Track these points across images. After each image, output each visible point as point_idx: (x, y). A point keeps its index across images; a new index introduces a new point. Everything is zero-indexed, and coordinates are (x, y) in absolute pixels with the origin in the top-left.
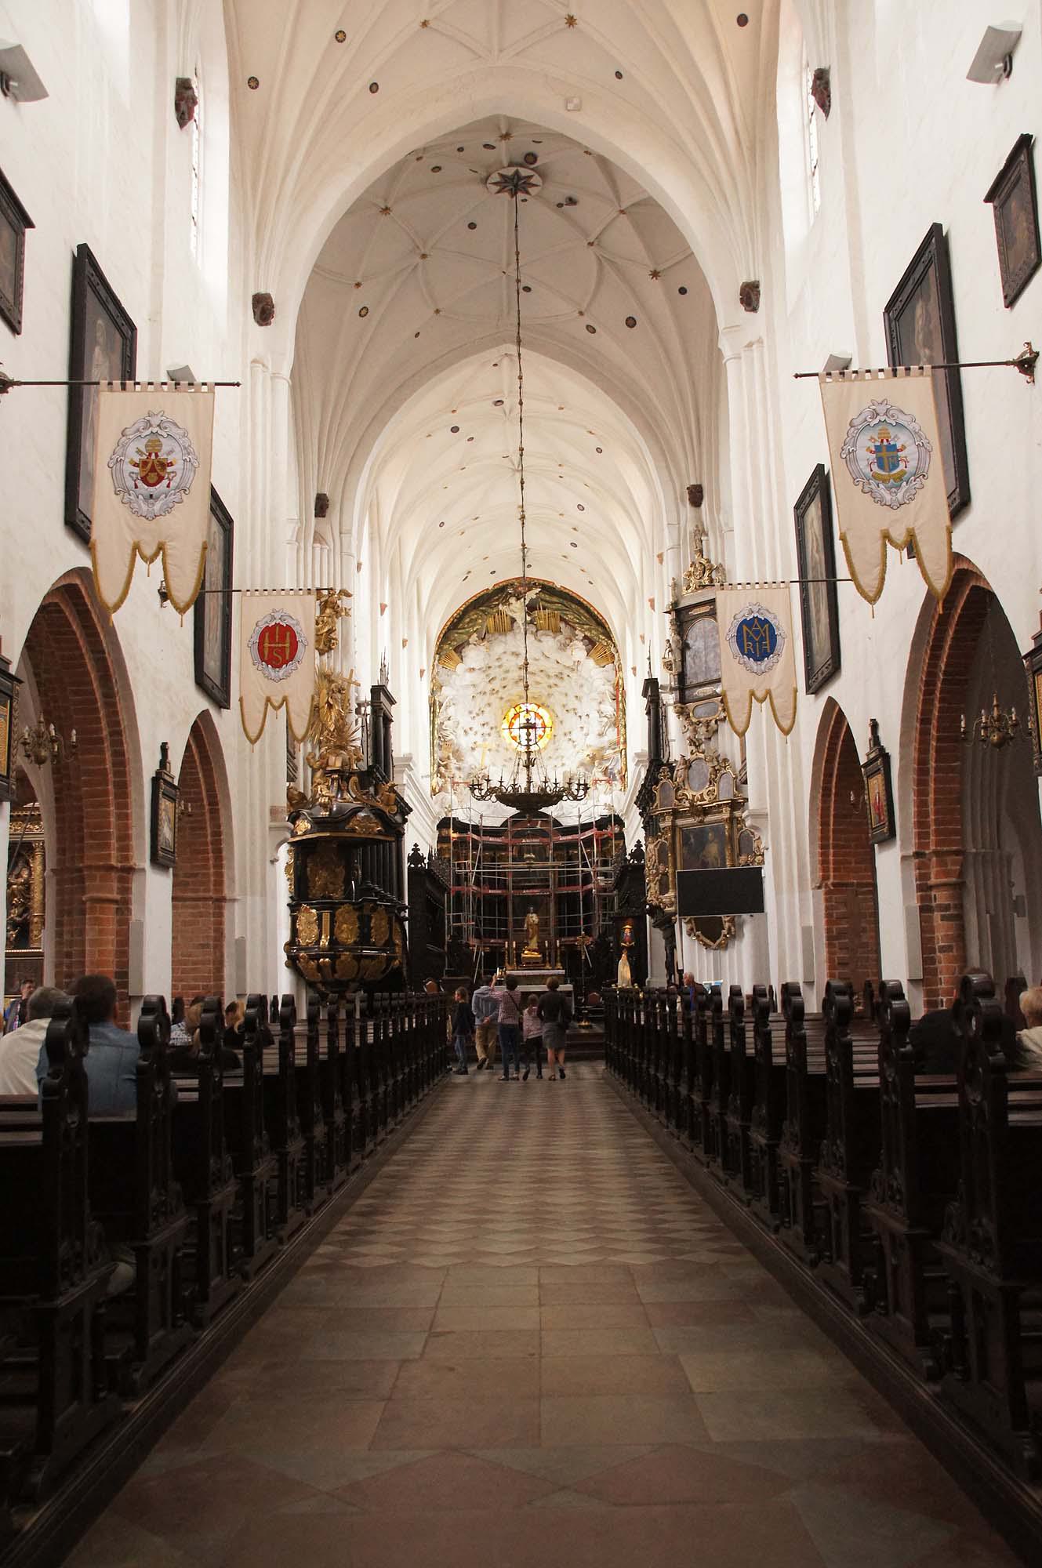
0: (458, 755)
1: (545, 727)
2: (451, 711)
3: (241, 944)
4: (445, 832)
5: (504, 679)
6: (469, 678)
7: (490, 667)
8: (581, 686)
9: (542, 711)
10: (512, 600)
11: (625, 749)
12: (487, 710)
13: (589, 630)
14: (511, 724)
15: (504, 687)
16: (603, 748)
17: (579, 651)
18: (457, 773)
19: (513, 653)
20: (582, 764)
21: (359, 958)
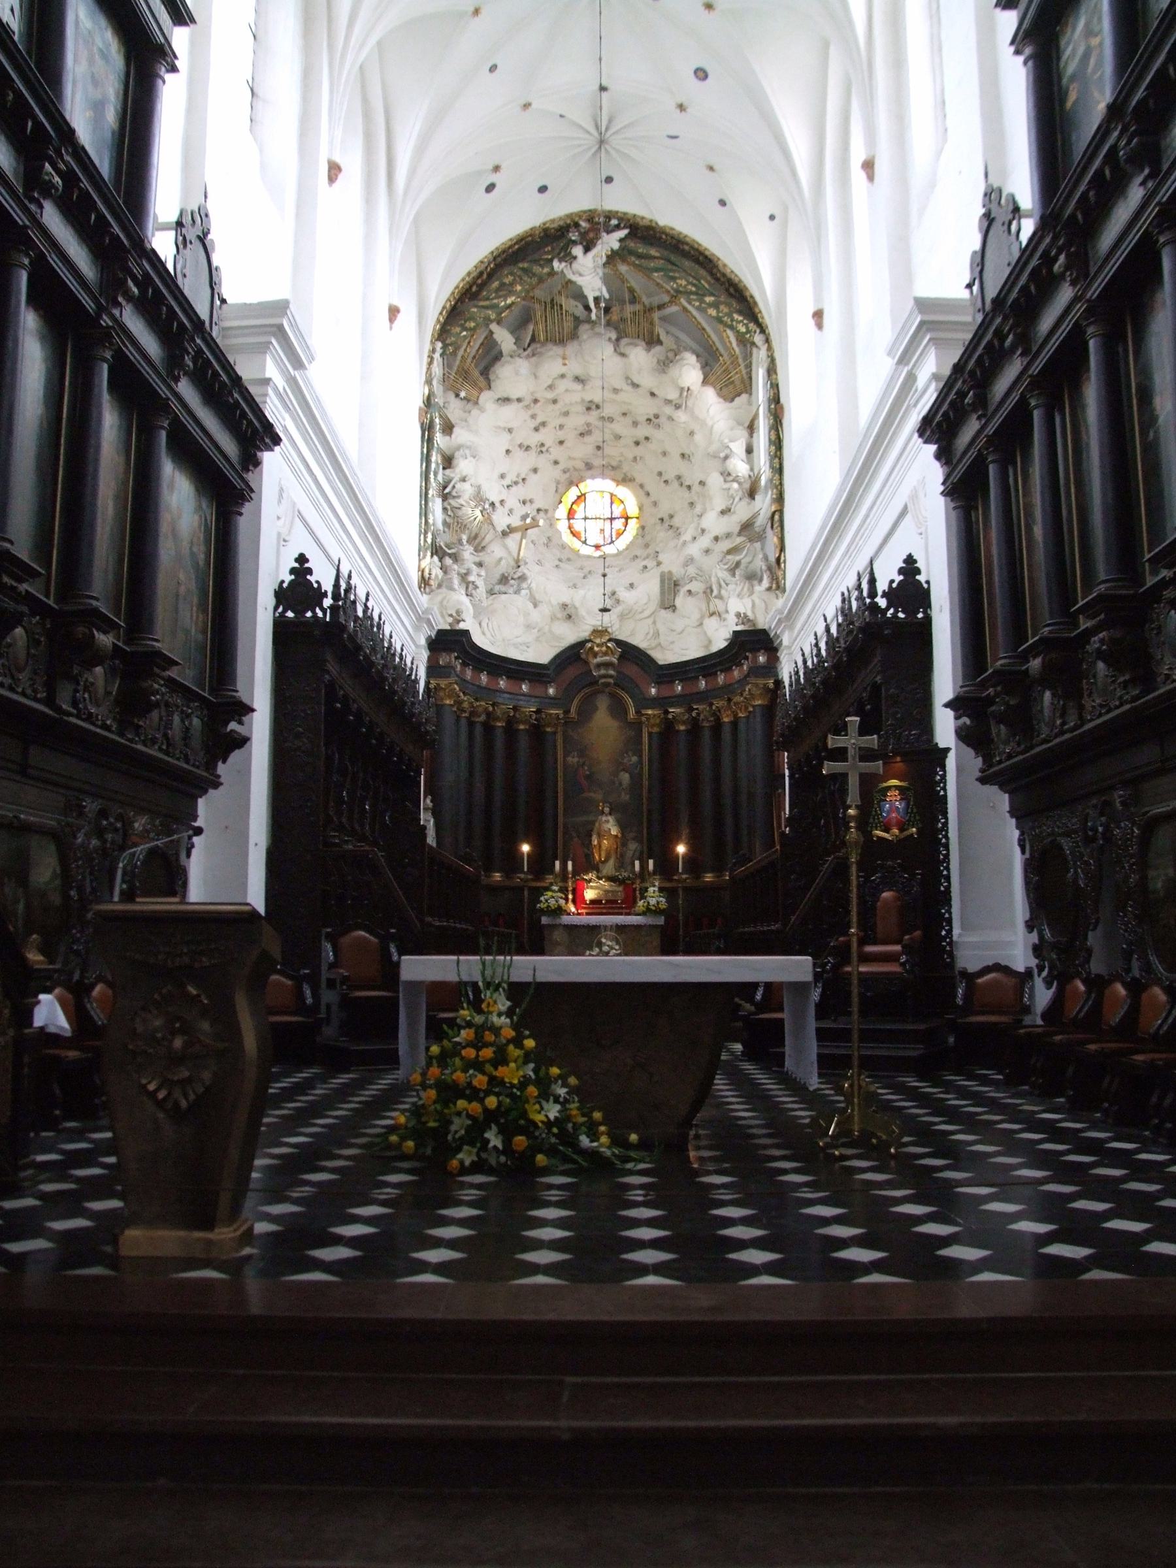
5: (561, 427)
7: (536, 401)
8: (692, 433)
9: (623, 492)
10: (577, 251)
11: (781, 511)
12: (533, 479)
13: (715, 305)
15: (561, 443)
17: (690, 373)
19: (577, 379)
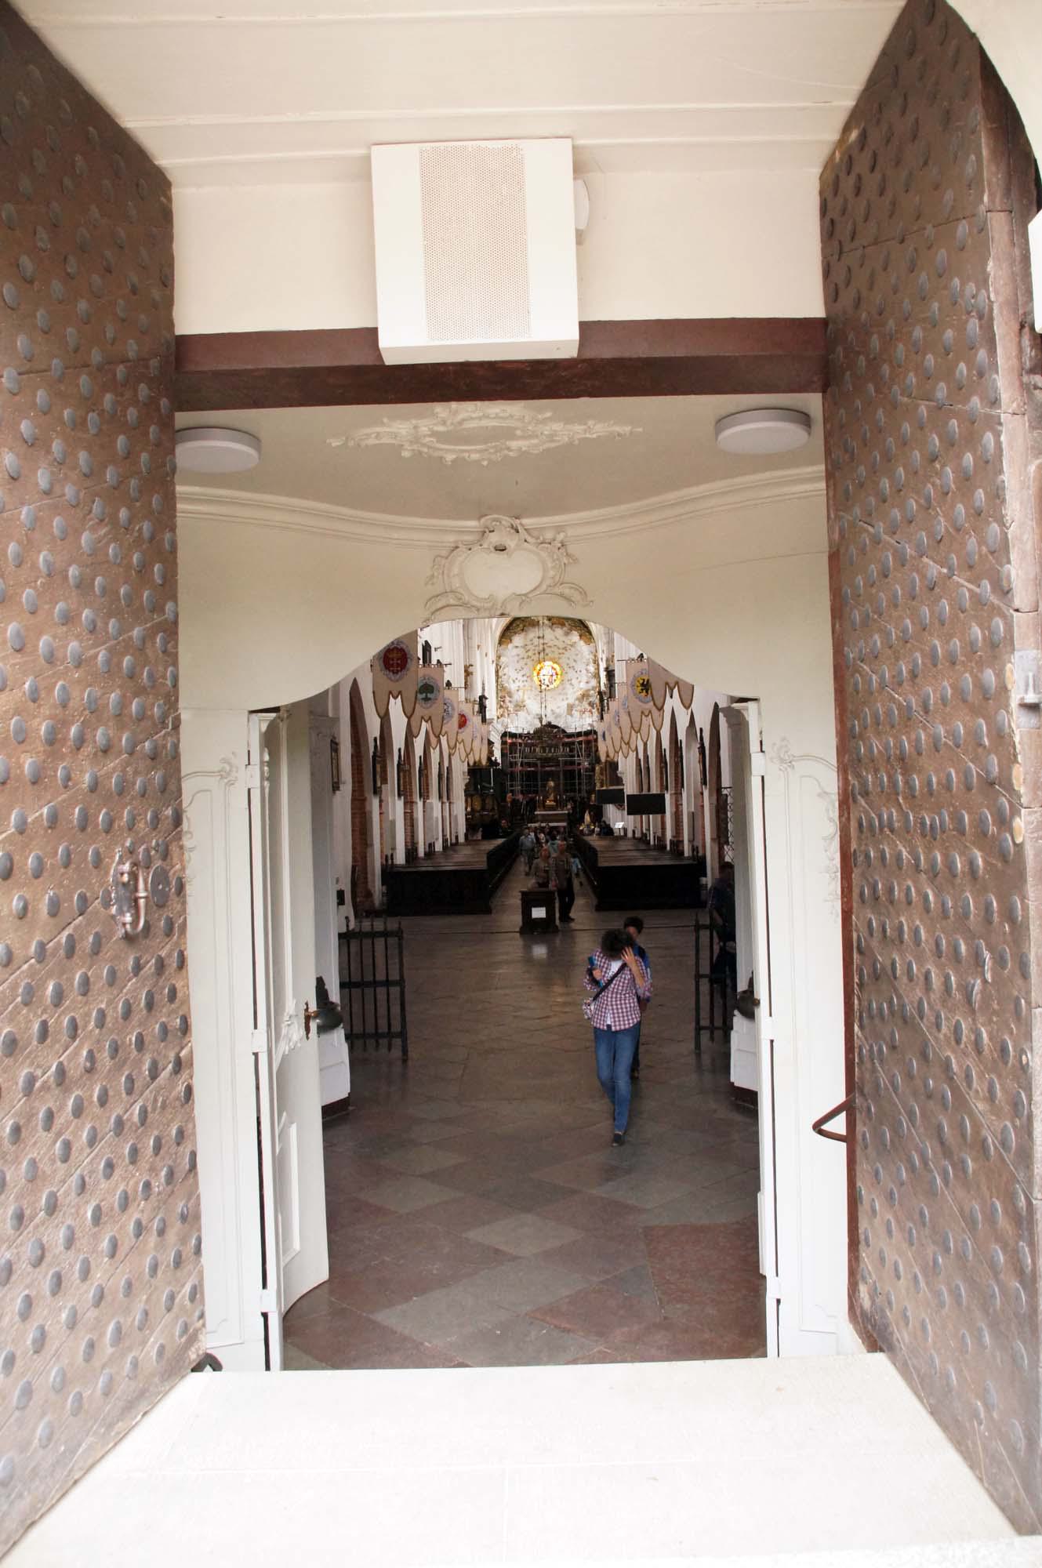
0: (510, 694)
1: (557, 674)
2: (506, 671)
3: (456, 816)
4: (504, 739)
6: (515, 651)
9: (555, 666)
12: (525, 667)
14: (538, 674)
16: (589, 690)
18: (509, 704)
20: (578, 699)
21: (482, 816)
